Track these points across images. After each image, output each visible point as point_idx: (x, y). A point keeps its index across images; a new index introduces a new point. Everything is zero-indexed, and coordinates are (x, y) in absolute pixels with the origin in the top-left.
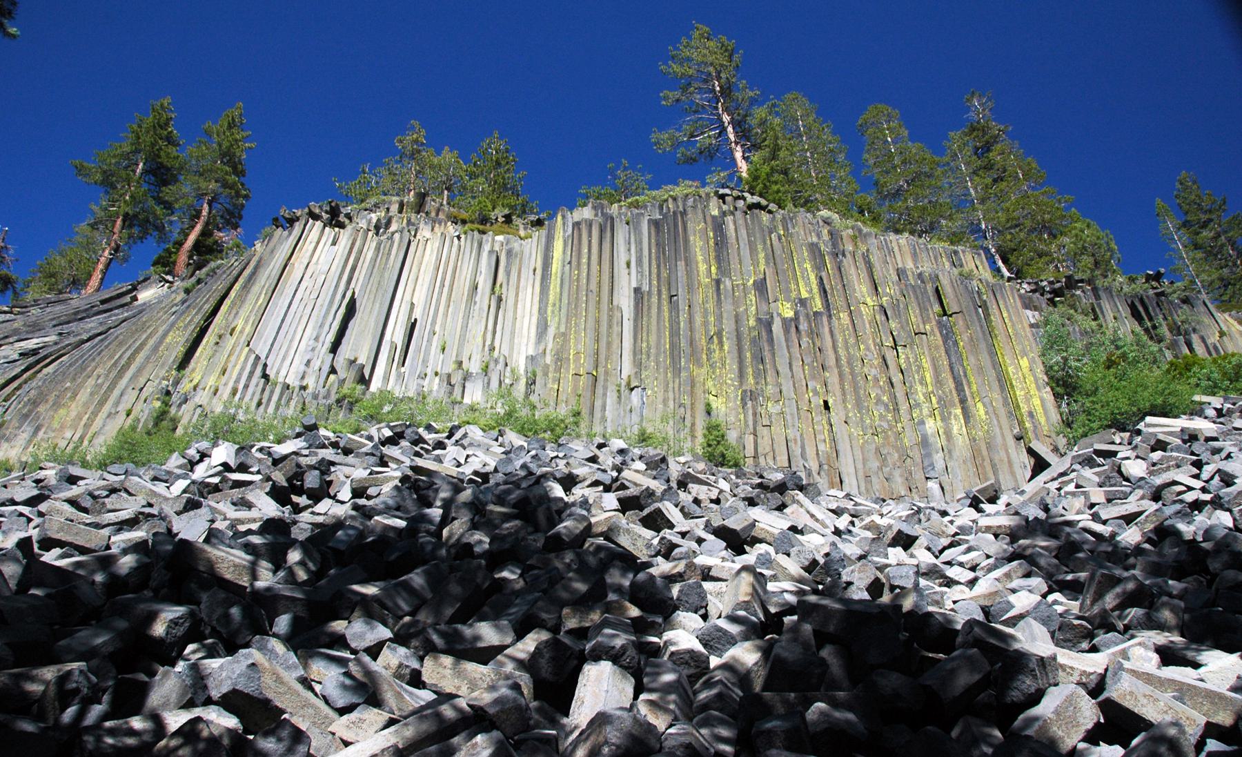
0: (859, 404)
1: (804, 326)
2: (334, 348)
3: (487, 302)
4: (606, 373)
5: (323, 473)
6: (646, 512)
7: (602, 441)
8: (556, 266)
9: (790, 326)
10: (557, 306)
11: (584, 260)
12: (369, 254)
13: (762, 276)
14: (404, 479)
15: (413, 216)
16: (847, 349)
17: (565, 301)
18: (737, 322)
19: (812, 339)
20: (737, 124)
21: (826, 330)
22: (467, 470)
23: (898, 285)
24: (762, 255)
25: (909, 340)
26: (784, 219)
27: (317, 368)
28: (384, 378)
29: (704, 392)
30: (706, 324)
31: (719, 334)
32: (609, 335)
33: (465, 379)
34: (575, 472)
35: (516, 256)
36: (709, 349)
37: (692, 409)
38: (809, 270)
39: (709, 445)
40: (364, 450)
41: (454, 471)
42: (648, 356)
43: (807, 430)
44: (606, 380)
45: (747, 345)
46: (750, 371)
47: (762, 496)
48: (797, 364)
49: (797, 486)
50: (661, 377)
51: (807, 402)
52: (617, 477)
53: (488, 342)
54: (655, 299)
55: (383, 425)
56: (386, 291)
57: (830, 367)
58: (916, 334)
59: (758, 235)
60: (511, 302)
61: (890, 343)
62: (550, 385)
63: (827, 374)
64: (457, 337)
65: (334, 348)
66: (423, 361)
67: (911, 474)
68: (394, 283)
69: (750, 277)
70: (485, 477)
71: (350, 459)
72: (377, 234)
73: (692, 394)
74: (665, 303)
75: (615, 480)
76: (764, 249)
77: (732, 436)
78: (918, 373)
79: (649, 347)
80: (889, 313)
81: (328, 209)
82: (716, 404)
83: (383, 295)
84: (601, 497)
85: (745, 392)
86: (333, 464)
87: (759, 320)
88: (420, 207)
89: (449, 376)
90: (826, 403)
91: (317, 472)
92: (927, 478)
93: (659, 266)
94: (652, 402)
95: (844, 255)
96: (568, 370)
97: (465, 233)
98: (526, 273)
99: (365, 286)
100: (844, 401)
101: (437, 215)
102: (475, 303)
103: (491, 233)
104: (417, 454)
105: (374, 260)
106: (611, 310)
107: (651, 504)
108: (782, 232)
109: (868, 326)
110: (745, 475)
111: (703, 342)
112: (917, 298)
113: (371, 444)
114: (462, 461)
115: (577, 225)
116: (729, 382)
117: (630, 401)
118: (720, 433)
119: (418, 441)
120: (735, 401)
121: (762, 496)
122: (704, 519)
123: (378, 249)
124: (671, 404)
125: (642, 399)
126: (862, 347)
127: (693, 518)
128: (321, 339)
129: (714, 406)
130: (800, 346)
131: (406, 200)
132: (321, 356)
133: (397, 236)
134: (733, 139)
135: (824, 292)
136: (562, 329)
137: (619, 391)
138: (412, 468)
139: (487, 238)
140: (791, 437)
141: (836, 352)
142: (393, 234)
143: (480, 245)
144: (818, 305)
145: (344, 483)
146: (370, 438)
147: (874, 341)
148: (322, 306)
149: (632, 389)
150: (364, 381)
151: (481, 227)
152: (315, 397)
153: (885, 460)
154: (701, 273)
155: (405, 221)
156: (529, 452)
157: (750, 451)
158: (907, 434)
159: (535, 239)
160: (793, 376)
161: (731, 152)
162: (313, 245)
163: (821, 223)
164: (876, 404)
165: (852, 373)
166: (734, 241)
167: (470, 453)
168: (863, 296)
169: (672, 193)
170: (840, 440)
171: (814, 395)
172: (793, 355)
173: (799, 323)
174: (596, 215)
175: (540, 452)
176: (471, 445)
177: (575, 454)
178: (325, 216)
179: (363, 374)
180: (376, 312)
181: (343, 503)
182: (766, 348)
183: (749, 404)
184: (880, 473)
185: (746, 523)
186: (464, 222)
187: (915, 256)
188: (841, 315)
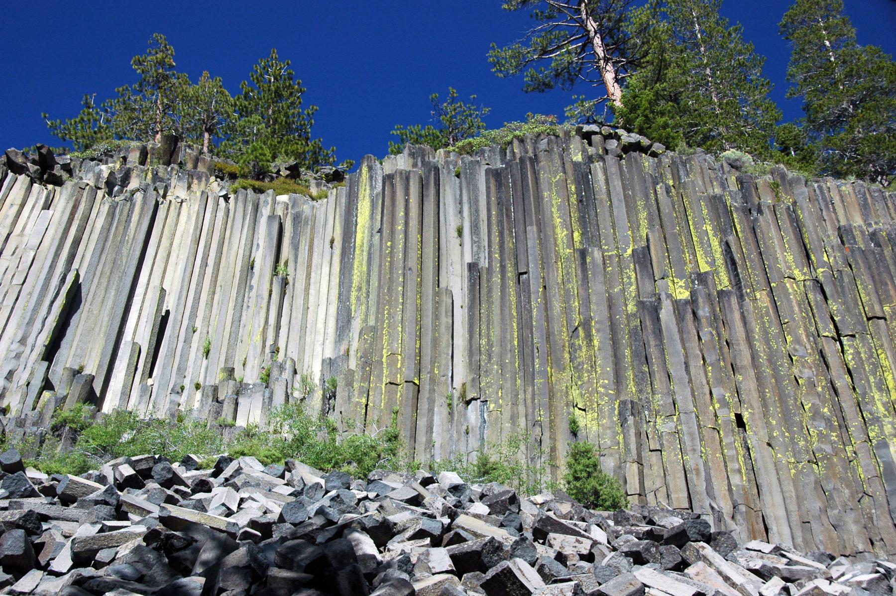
0: (787, 419)
1: (704, 312)
2: (50, 353)
3: (267, 286)
4: (433, 380)
5: (29, 533)
6: (491, 573)
7: (428, 475)
8: (361, 236)
9: (685, 312)
10: (364, 290)
11: (400, 227)
12: (98, 221)
13: (643, 244)
14: (151, 536)
15: (161, 169)
16: (767, 341)
17: (374, 283)
18: (610, 307)
19: (717, 329)
20: (607, 33)
21: (737, 315)
22: (242, 520)
23: (840, 251)
24: (643, 215)
25: (859, 328)
26: (673, 165)
27: (23, 382)
28: (123, 393)
29: (567, 405)
30: (567, 311)
31: (586, 324)
32: (435, 329)
33: (237, 394)
34: (392, 518)
35: (306, 222)
36: (572, 345)
37: (551, 428)
38: (711, 233)
39: (577, 479)
40: (92, 496)
41: (222, 522)
42: (490, 357)
44: (432, 391)
45: (625, 339)
46: (630, 374)
47: (653, 550)
48: (696, 364)
49: (703, 535)
50: (508, 385)
51: (712, 416)
52: (450, 524)
53: (270, 342)
54: (497, 279)
55: (121, 459)
56: (124, 273)
57: (743, 367)
58: (869, 319)
59: (637, 188)
60: (300, 285)
61: (830, 331)
62: (355, 399)
63: (740, 378)
64: (227, 335)
65: (50, 353)
66: (179, 369)
67: (871, 519)
68: (135, 262)
69: (628, 246)
70: (266, 529)
71: (72, 510)
72: (110, 193)
73: (551, 407)
74: (511, 283)
75: (447, 529)
76: (647, 206)
77: (608, 465)
78: (874, 374)
79: (490, 344)
80: (827, 290)
81: (37, 157)
82: (584, 420)
83: (121, 279)
84: (428, 554)
85: (623, 403)
86: (46, 518)
87: (641, 304)
88: (171, 157)
89: (215, 389)
90: (739, 417)
91: (21, 532)
93: (501, 234)
94: (497, 418)
95: (760, 211)
96: (380, 378)
97: (235, 192)
98: (321, 246)
99: (92, 268)
100: (766, 414)
101: (195, 167)
102: (251, 288)
103: (270, 191)
104: (170, 500)
105: (106, 229)
106: (437, 294)
107: (497, 562)
108: (671, 183)
109: (796, 309)
110: (627, 519)
112: (870, 268)
113: (103, 488)
114: (234, 508)
115: (389, 179)
116: (601, 390)
117: (464, 415)
118: (591, 461)
119: (173, 480)
120: (610, 417)
121: (653, 550)
122: (572, 583)
123: (111, 214)
124: (522, 422)
125: (482, 416)
126: (789, 338)
127: (555, 582)
128: (30, 341)
129: (581, 423)
130: (700, 338)
131: (150, 146)
132: (30, 365)
133: (139, 196)
134: (601, 55)
135: (732, 263)
136: (372, 322)
137: (449, 405)
138: (162, 519)
139: (266, 199)
140: (690, 465)
141: (751, 346)
142: (133, 193)
143: (256, 208)
144: (724, 281)
145: (63, 545)
146: (102, 479)
147: (806, 330)
148: (30, 294)
149: (468, 403)
150: (94, 399)
151: (257, 184)
152: (21, 423)
153: (830, 499)
154: (559, 241)
155: (150, 175)
156: (327, 492)
157: (633, 485)
158: (862, 462)
159: (332, 199)
160: (690, 381)
161: (599, 73)
162: (15, 209)
163: (727, 168)
164: (813, 418)
165: (776, 375)
166: (604, 197)
167: (245, 495)
168: (789, 268)
169: (517, 133)
170: (762, 471)
171: (722, 406)
173: (697, 306)
174: (415, 165)
175: (344, 492)
176: (247, 484)
177: (390, 494)
178: (32, 168)
179: (92, 391)
180: (109, 303)
181: (58, 575)
182: (652, 343)
183: (631, 420)
184: (824, 518)
185: (632, 589)
186: (233, 176)
187: (865, 208)
188: (758, 295)
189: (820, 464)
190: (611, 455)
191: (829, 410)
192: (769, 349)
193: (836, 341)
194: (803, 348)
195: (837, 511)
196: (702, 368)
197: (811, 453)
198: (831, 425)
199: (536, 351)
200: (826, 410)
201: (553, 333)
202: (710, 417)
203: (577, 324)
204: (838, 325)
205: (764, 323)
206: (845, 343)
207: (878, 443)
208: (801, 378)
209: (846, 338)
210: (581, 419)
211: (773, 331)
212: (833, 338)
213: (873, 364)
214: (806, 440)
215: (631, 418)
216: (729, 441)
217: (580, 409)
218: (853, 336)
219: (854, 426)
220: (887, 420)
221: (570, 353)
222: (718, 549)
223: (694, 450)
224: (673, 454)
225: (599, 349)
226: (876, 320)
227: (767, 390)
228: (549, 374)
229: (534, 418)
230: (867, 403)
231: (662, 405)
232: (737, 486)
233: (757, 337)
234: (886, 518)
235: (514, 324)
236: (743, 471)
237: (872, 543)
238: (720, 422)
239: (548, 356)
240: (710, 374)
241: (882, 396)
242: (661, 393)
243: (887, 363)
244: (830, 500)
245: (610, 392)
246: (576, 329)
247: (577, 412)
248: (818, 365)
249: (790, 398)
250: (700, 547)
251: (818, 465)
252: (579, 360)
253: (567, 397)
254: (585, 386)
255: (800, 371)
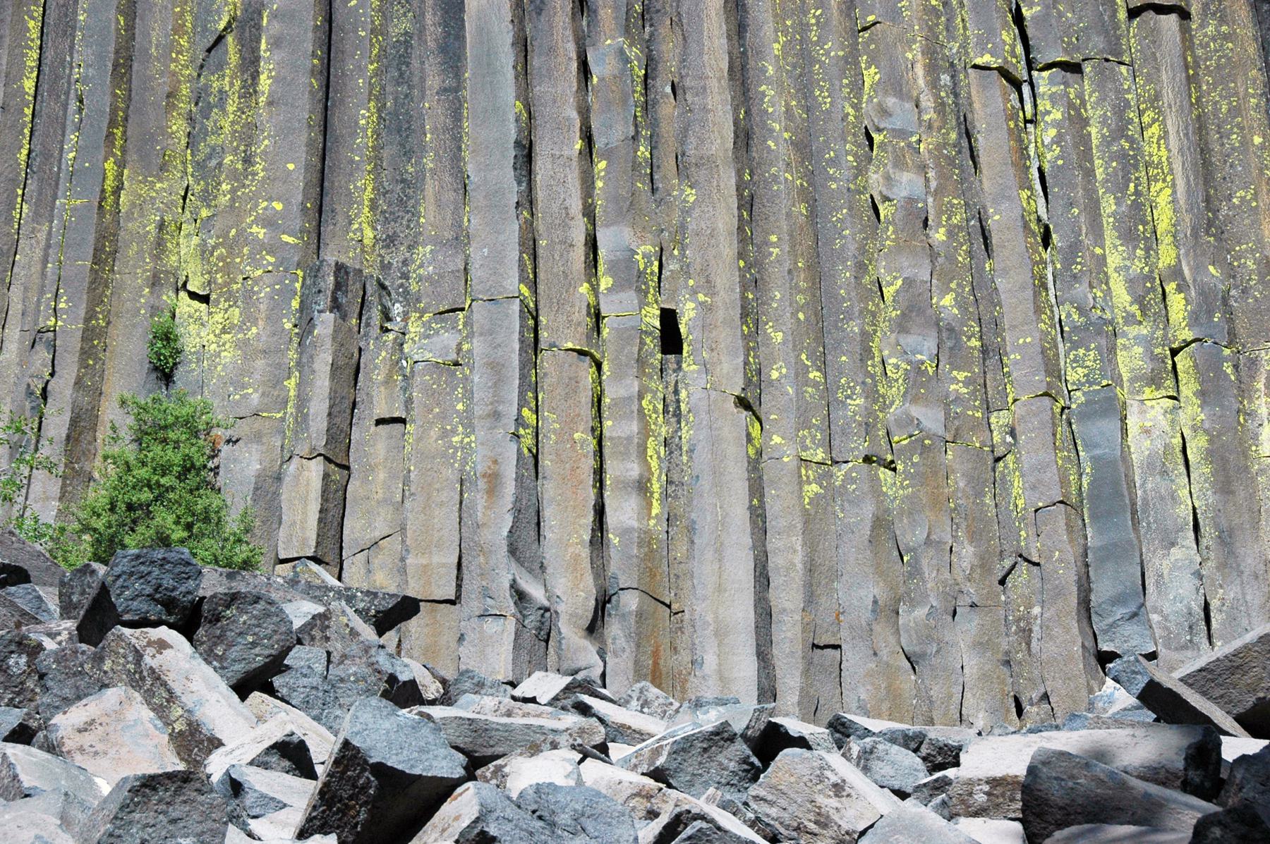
16: (805, 89)
43: (565, 434)
46: (364, 187)
49: (169, 604)
57: (706, 162)
58: (1133, 13)
63: (691, 195)
67: (1026, 634)
90: (669, 319)
92: (1105, 658)
111: (183, 65)
116: (260, 232)
120: (273, 319)
126: (871, 75)
130: (585, 70)
164: (902, 326)
165: (812, 196)
170: (705, 483)
172: (544, 113)
182: (434, 81)
189: (900, 467)
190: (258, 437)
191: (960, 303)
192: (808, 110)
193: (1016, 84)
194: (909, 106)
195: (926, 610)
196: (575, 163)
197: (882, 433)
198: (957, 348)
199: (73, 105)
200: (948, 300)
201: (146, 51)
202: (576, 317)
203: (222, 25)
204: (1030, 32)
205: (804, 28)
206: (1041, 89)
207: (1088, 403)
208: (886, 199)
209: (1046, 74)
210: (193, 328)
211: (827, 53)
212: (1004, 73)
213: (1122, 156)
214: (872, 394)
215: (329, 317)
216: (622, 393)
217: (193, 296)
218: (1074, 68)
219: (1018, 348)
220: (1133, 331)
221: (191, 119)
222: (219, 651)
223: (496, 415)
224: (435, 432)
225: (270, 103)
226: (1150, 14)
227: (774, 238)
228: (110, 184)
229: (36, 323)
230: (1075, 277)
231: (429, 278)
232: (625, 532)
233: (771, 70)
234: (1068, 631)
235: (31, 24)
236: (655, 487)
237: (1020, 711)
238: (605, 332)
239: (113, 123)
240: (599, 184)
241: (1131, 257)
242: (435, 241)
243: (1163, 152)
244: (911, 575)
245: (286, 238)
246: (220, 39)
247: (185, 305)
248: (951, 161)
249: (844, 262)
250: (150, 644)
251: (894, 470)
252: (212, 140)
253: (157, 258)
254: (219, 224)
255: (888, 178)
